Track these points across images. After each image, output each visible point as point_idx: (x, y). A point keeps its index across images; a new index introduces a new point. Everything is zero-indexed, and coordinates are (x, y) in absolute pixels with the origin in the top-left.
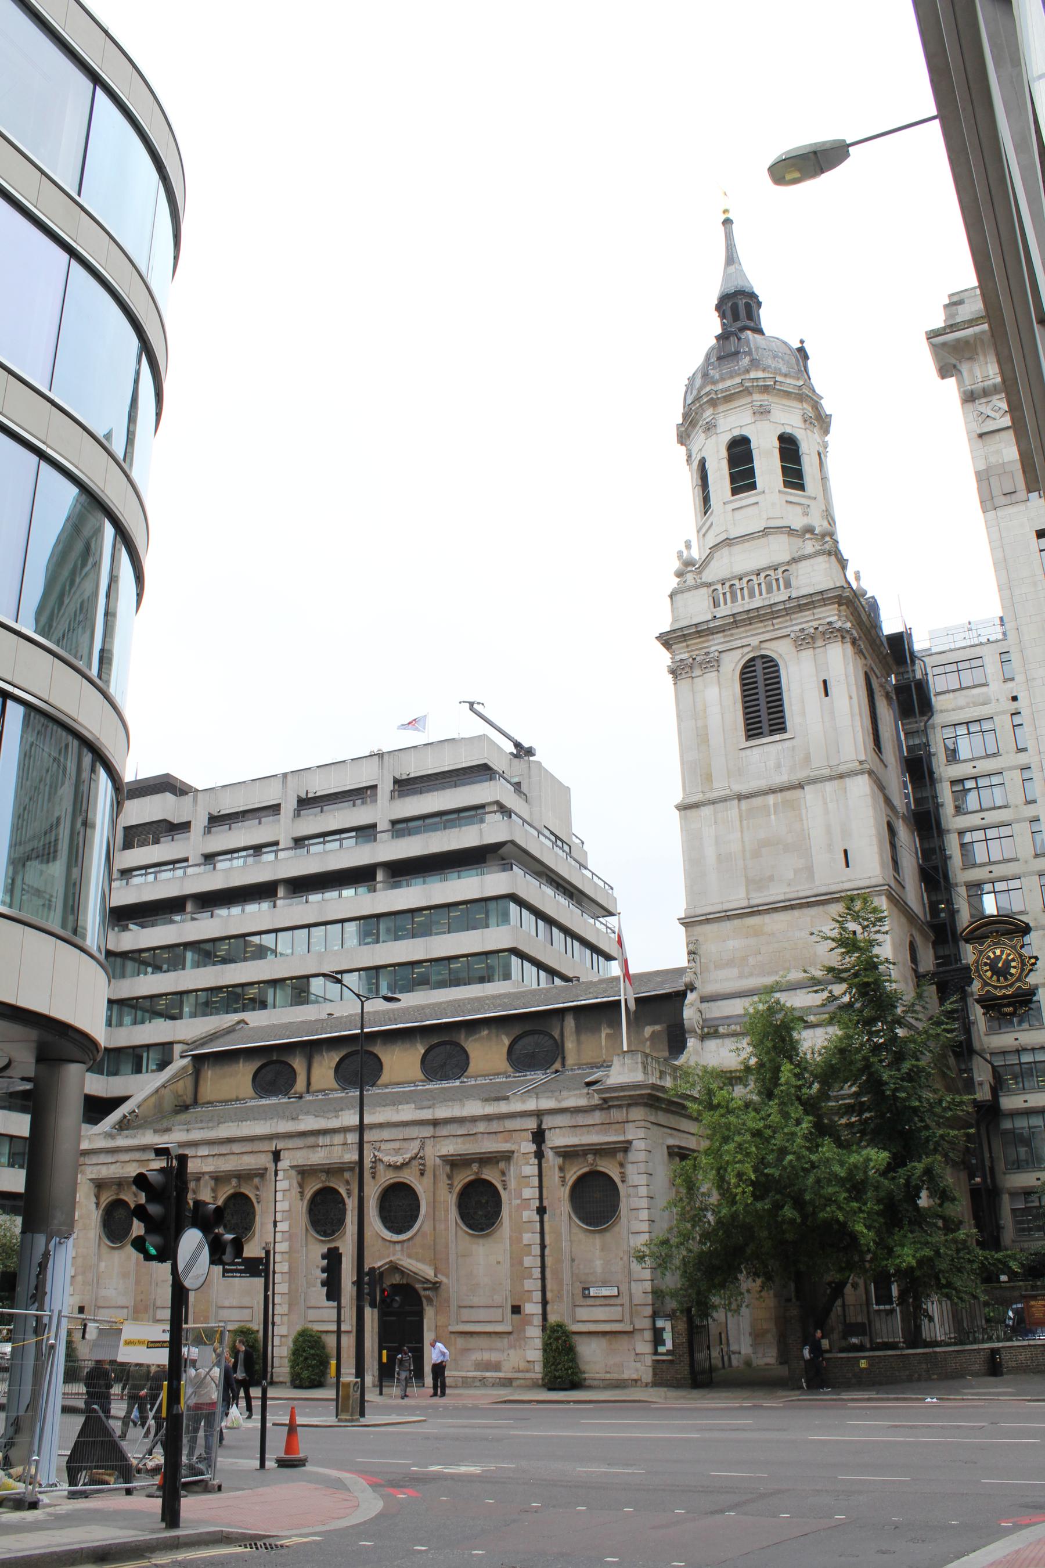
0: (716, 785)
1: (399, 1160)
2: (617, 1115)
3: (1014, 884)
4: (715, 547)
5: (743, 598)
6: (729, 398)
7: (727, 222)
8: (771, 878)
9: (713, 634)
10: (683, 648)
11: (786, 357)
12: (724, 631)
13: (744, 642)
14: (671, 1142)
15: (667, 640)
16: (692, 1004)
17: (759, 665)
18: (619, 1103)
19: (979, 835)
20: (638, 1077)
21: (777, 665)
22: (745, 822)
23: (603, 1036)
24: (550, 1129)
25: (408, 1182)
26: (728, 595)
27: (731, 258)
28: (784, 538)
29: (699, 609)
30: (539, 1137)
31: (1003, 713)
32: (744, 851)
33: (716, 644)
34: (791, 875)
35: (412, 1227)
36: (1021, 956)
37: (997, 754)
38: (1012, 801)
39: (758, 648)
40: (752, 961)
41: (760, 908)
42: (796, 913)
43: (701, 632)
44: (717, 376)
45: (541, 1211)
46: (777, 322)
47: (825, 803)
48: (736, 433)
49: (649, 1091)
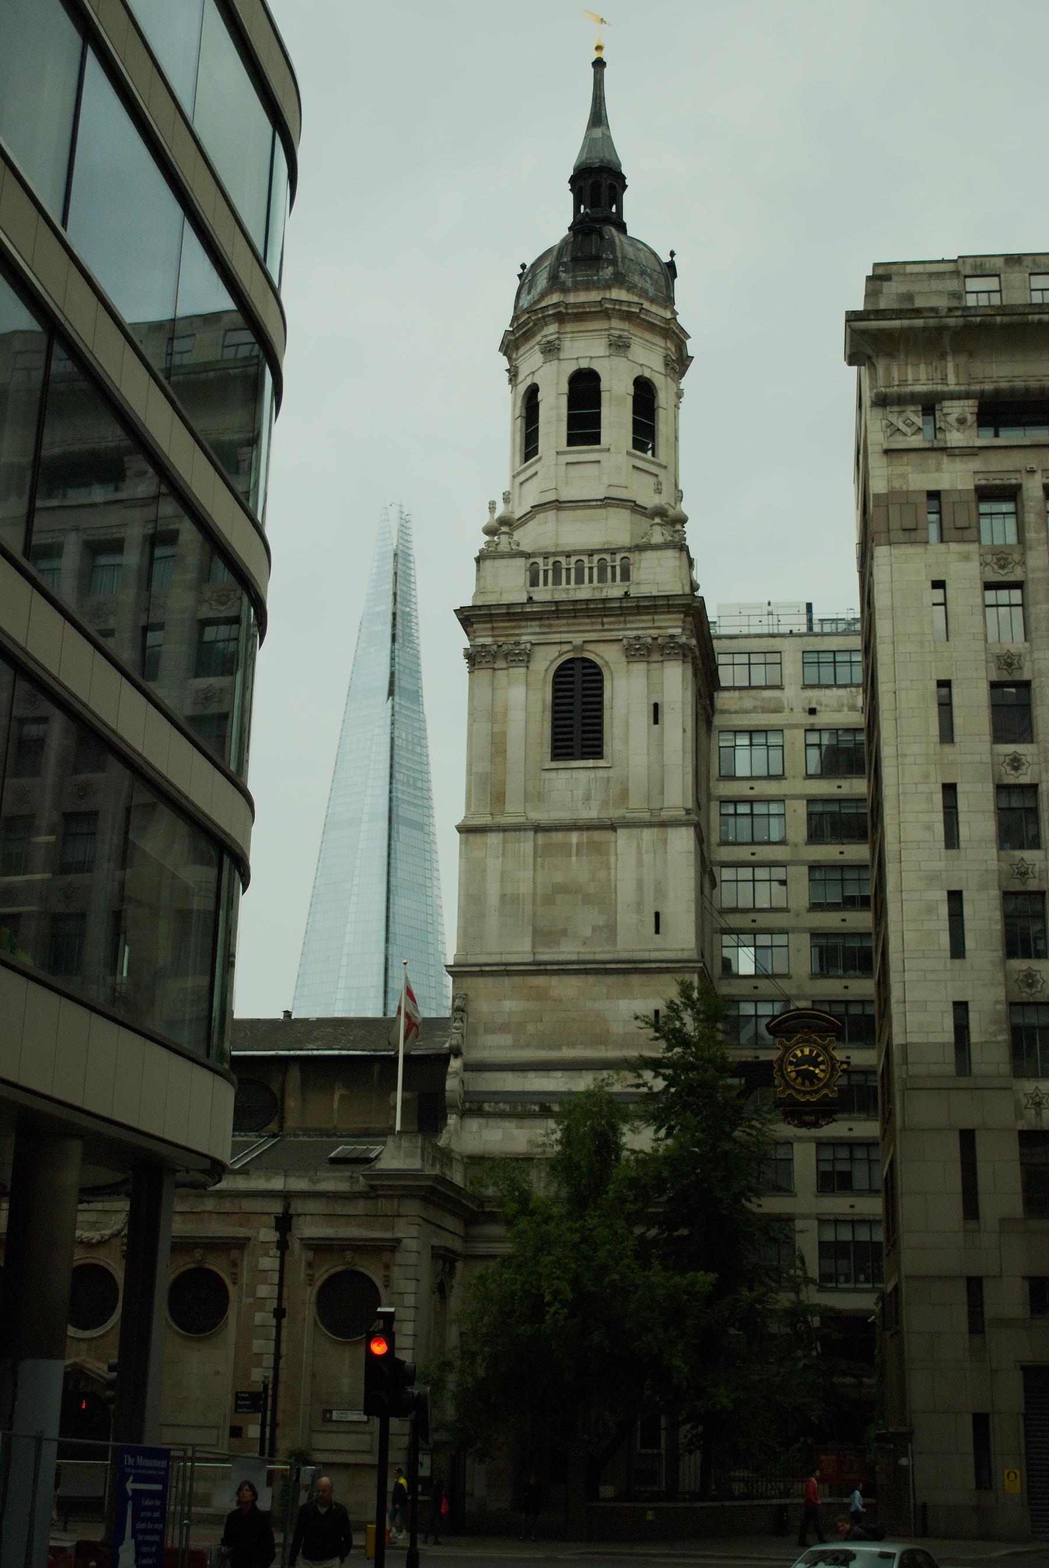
0: (509, 808)
1: (95, 1236)
2: (386, 1206)
3: (780, 939)
4: (538, 508)
5: (568, 582)
6: (581, 315)
7: (599, 64)
8: (564, 932)
9: (527, 620)
10: (486, 629)
11: (655, 276)
12: (540, 619)
13: (565, 637)
14: (435, 1242)
15: (467, 617)
16: (456, 1073)
17: (578, 671)
18: (390, 1192)
19: (746, 873)
20: (415, 1163)
21: (600, 673)
22: (539, 860)
23: (337, 1097)
24: (299, 1215)
25: (105, 1265)
26: (550, 574)
27: (598, 117)
28: (625, 515)
29: (511, 585)
30: (284, 1223)
31: (796, 726)
32: (535, 894)
33: (528, 634)
34: (588, 932)
35: (106, 1321)
36: (832, 1058)
37: (781, 777)
38: (791, 837)
39: (580, 648)
40: (530, 1029)
41: (549, 967)
42: (591, 979)
43: (512, 615)
44: (569, 283)
45: (279, 1313)
46: (645, 217)
47: (639, 853)
48: (584, 364)
49: (430, 1183)
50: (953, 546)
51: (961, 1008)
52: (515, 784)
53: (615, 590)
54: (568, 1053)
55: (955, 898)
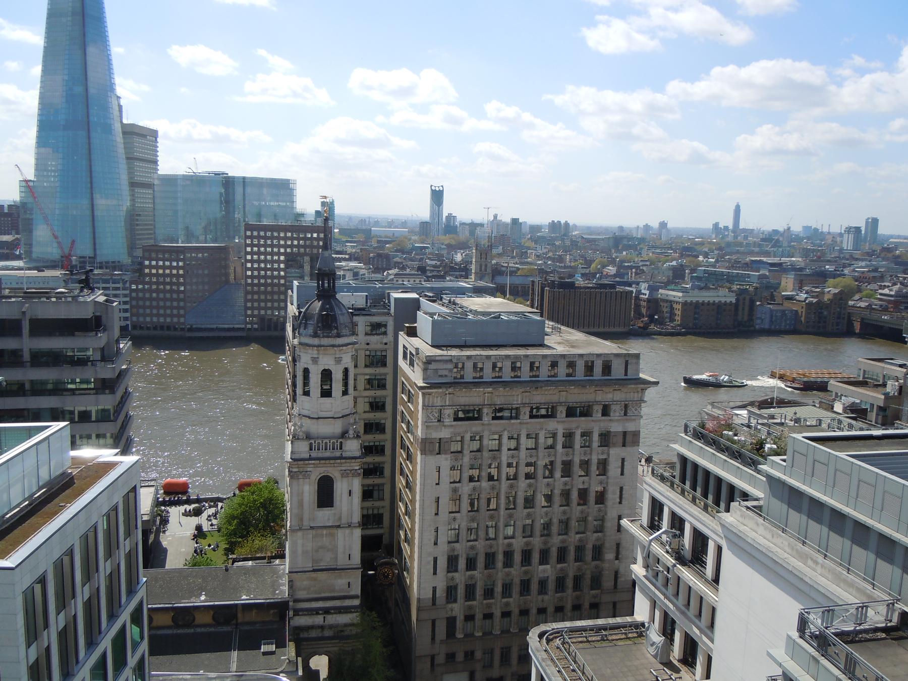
50: (443, 456)
51: (434, 589)
52: (306, 517)
53: (337, 454)
54: (323, 595)
55: (435, 560)
